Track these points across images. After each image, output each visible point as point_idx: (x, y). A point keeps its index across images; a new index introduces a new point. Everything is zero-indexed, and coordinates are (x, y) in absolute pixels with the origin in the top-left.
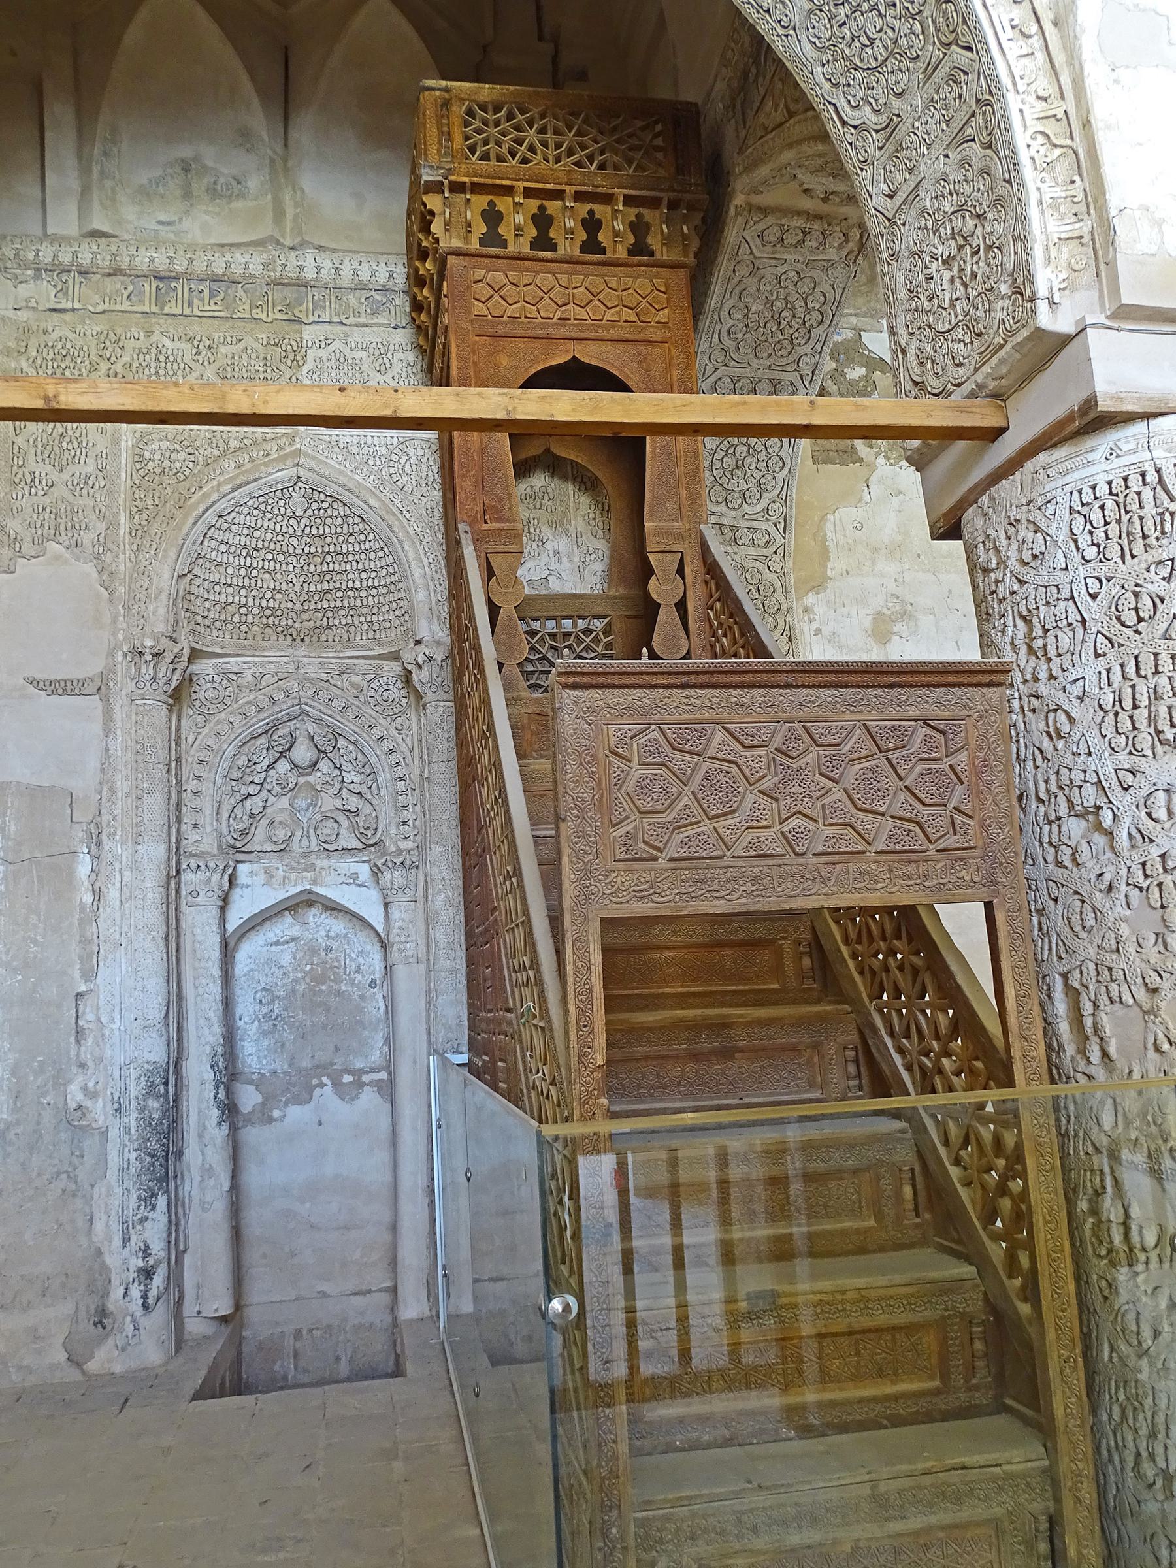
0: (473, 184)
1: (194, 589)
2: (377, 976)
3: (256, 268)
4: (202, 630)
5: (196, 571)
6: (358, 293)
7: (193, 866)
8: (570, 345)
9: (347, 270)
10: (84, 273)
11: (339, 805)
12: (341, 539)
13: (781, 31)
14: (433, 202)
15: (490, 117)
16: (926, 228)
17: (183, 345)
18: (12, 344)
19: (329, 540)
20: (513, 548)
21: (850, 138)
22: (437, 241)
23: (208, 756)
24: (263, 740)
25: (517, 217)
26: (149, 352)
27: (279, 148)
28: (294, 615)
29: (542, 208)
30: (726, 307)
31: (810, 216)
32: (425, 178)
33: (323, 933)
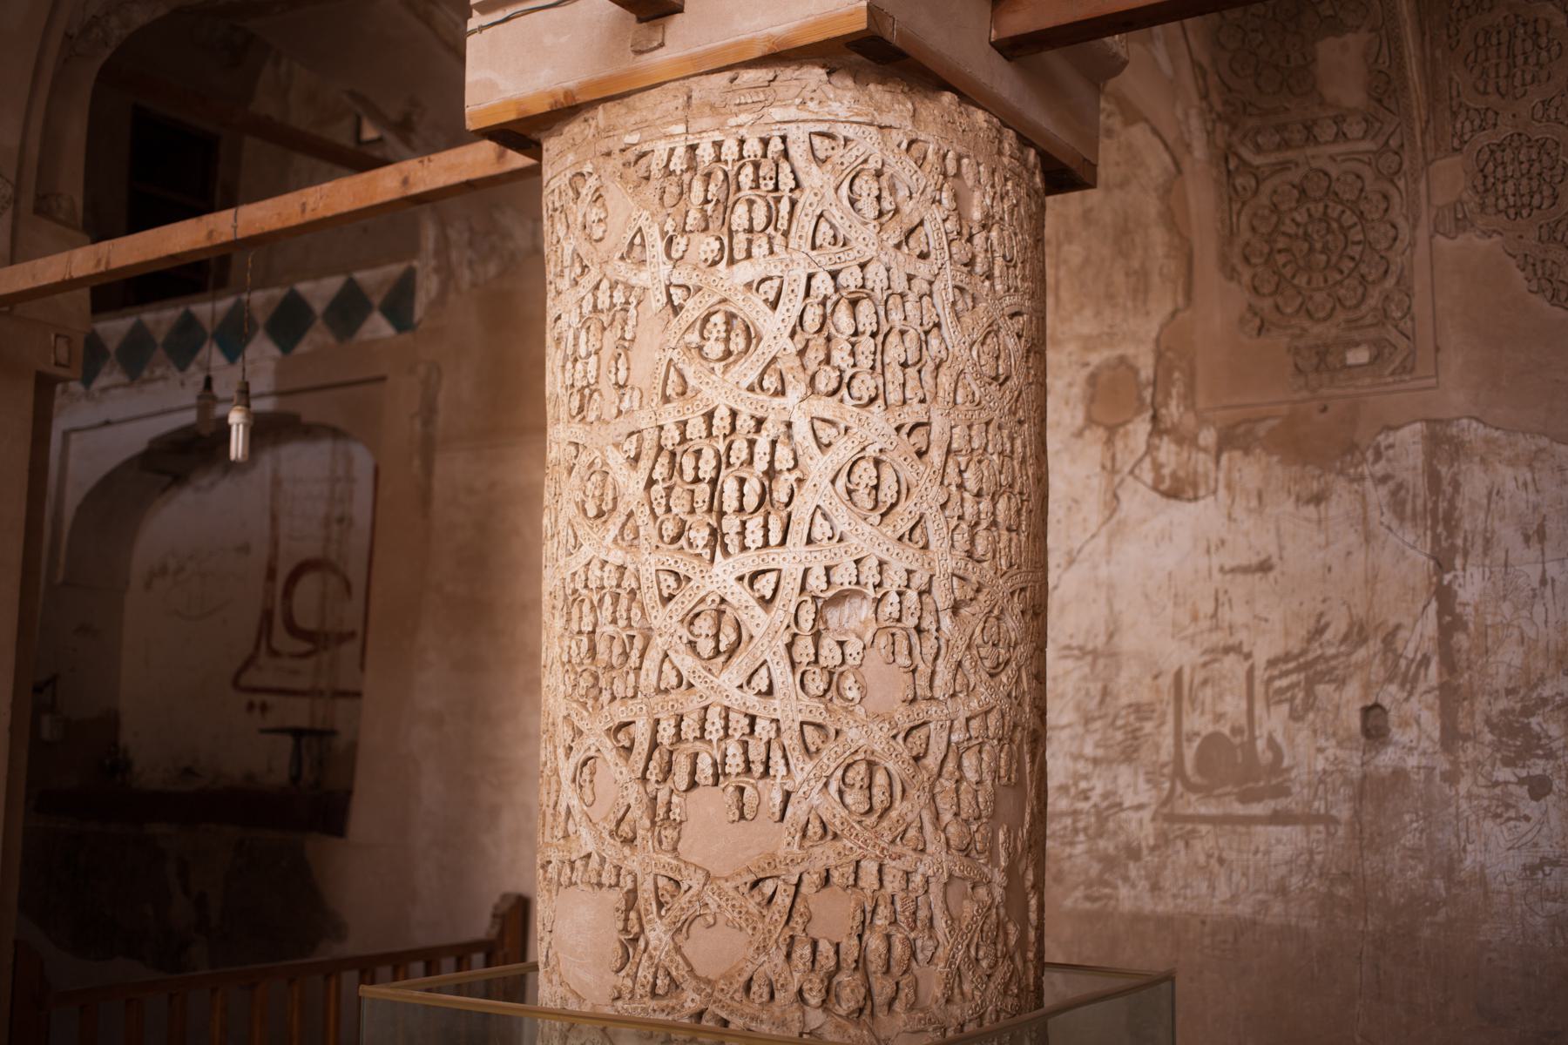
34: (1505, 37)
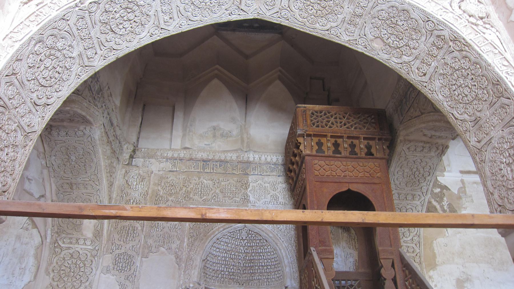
0: (314, 134)
1: (207, 265)
3: (234, 158)
4: (208, 280)
5: (208, 258)
6: (266, 165)
8: (347, 185)
9: (263, 158)
10: (181, 160)
13: (430, 92)
14: (300, 140)
15: (319, 115)
16: (496, 153)
17: (210, 182)
18: (157, 182)
19: (254, 248)
20: (331, 257)
21: (459, 123)
22: (302, 152)
25: (328, 144)
26: (199, 184)
27: (243, 123)
29: (336, 141)
30: (396, 171)
31: (425, 142)
32: (298, 133)
34: (127, 229)
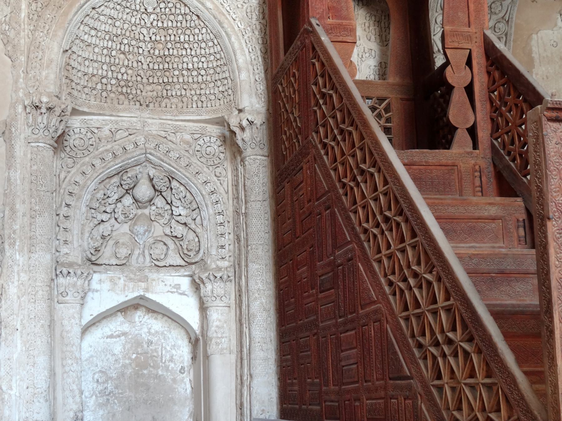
2: (186, 364)
4: (75, 93)
7: (65, 271)
11: (168, 231)
12: (180, 31)
19: (170, 31)
20: (349, 39)
23: (76, 190)
24: (116, 180)
28: (141, 86)
33: (146, 330)
